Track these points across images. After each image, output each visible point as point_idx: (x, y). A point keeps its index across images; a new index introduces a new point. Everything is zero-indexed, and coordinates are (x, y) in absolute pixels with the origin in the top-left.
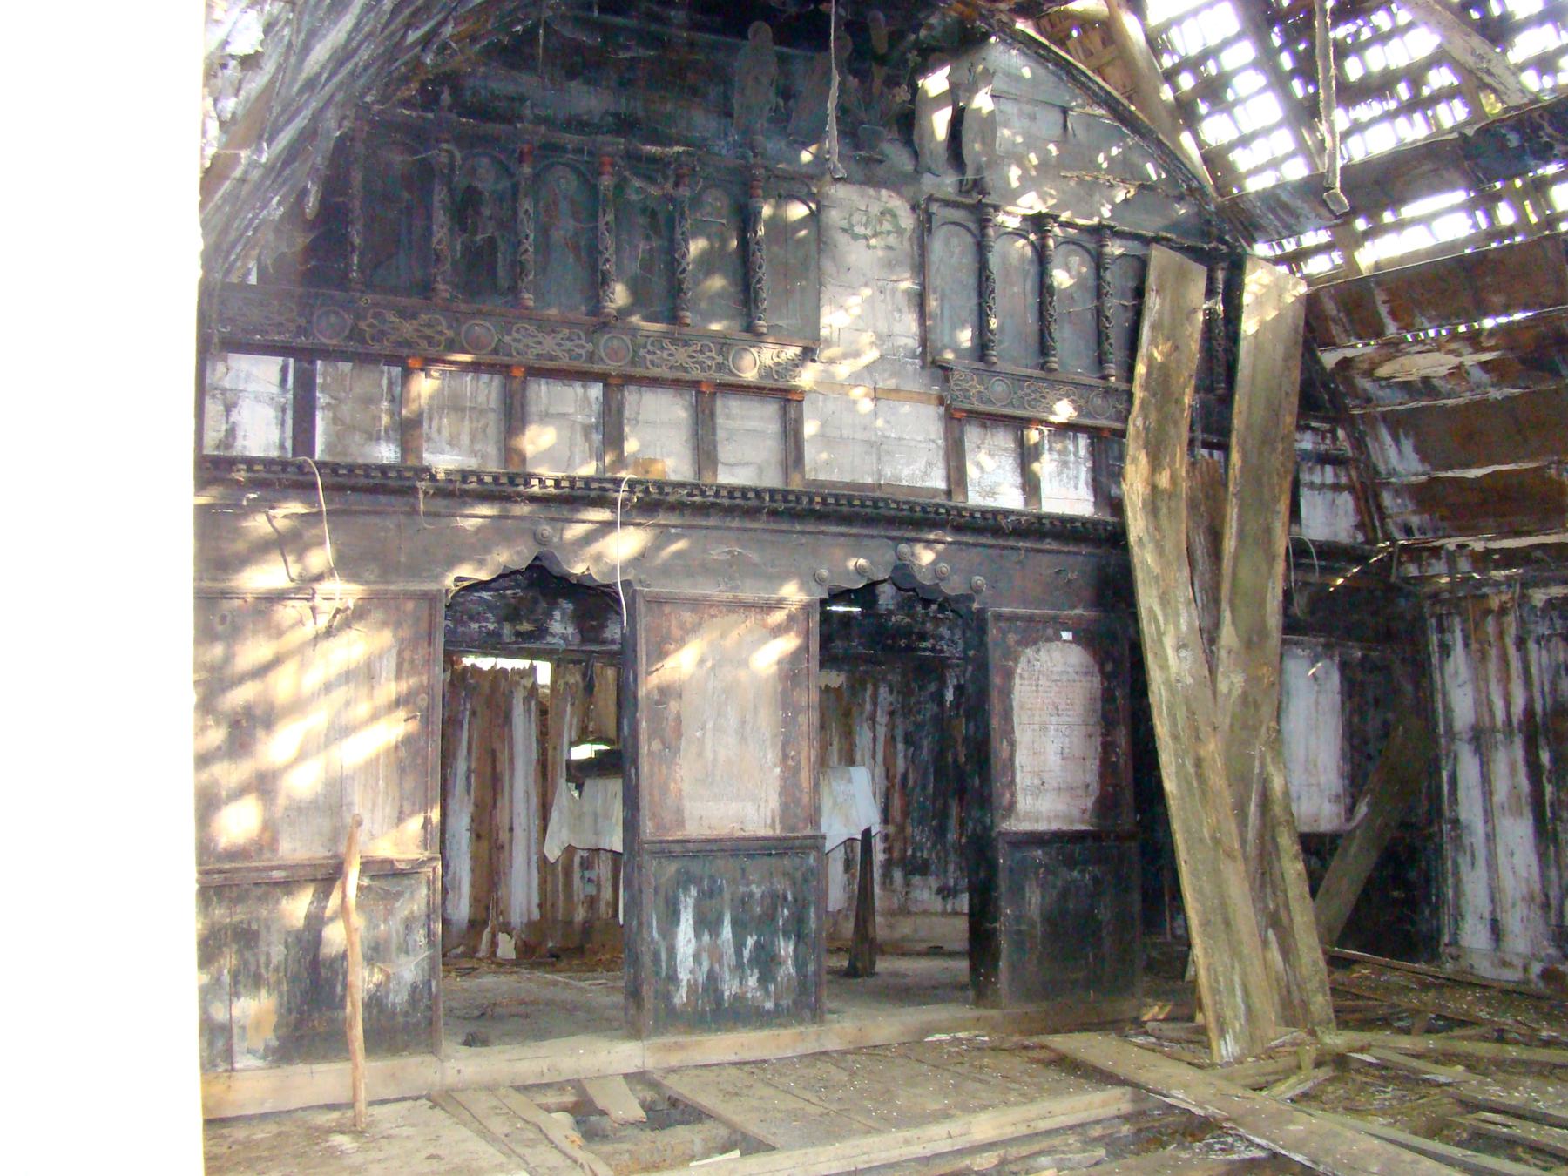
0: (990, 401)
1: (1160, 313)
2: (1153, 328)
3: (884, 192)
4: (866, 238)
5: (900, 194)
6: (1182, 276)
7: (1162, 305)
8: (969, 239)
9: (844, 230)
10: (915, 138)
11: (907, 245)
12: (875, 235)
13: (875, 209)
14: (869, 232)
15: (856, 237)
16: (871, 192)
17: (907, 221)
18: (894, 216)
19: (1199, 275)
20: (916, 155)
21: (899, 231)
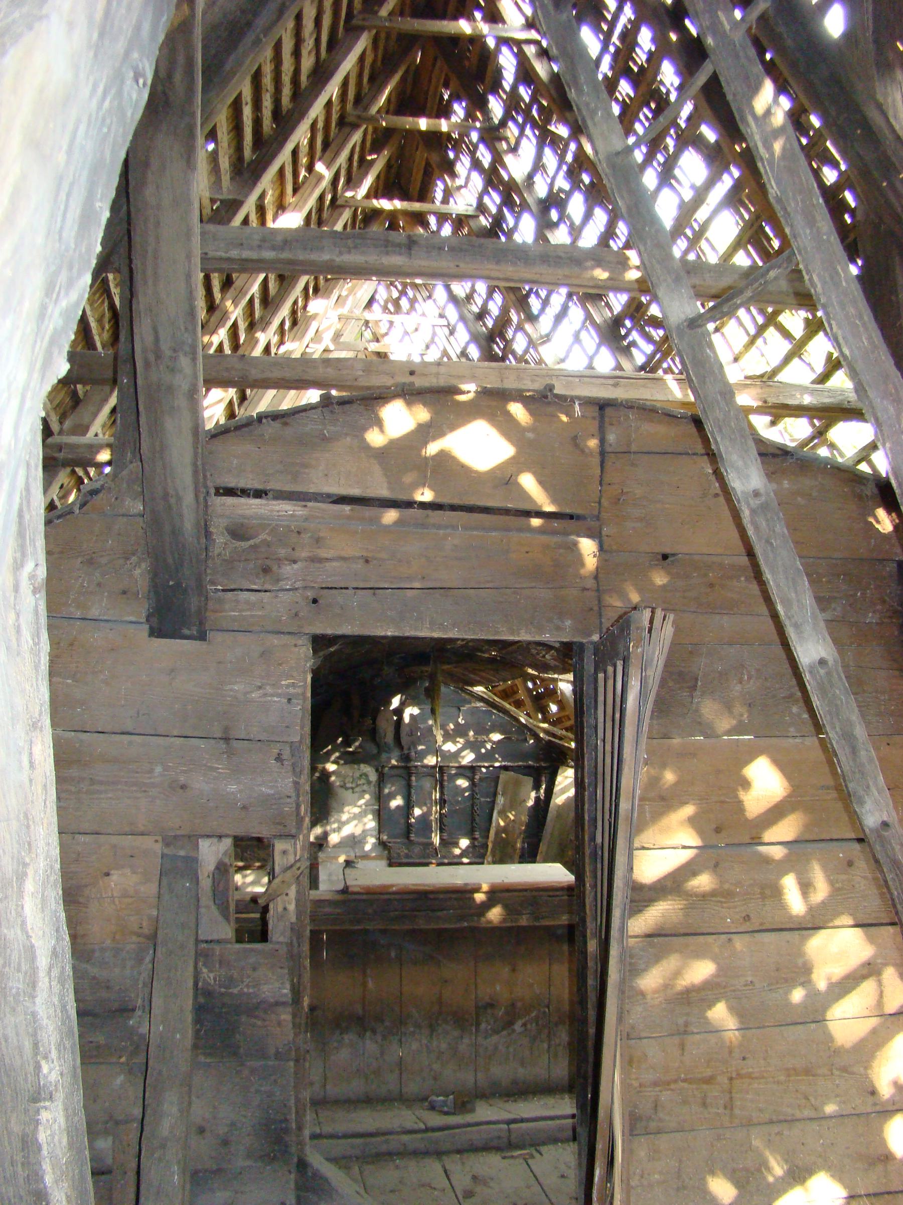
0: (411, 857)
1: (504, 805)
2: (499, 813)
3: (362, 766)
4: (352, 788)
5: (369, 764)
6: (517, 784)
7: (505, 799)
8: (404, 782)
9: (342, 787)
10: (377, 739)
11: (372, 788)
12: (357, 786)
13: (357, 774)
14: (354, 786)
15: (347, 789)
16: (356, 766)
17: (373, 777)
18: (366, 775)
19: (529, 781)
20: (378, 746)
21: (369, 783)
